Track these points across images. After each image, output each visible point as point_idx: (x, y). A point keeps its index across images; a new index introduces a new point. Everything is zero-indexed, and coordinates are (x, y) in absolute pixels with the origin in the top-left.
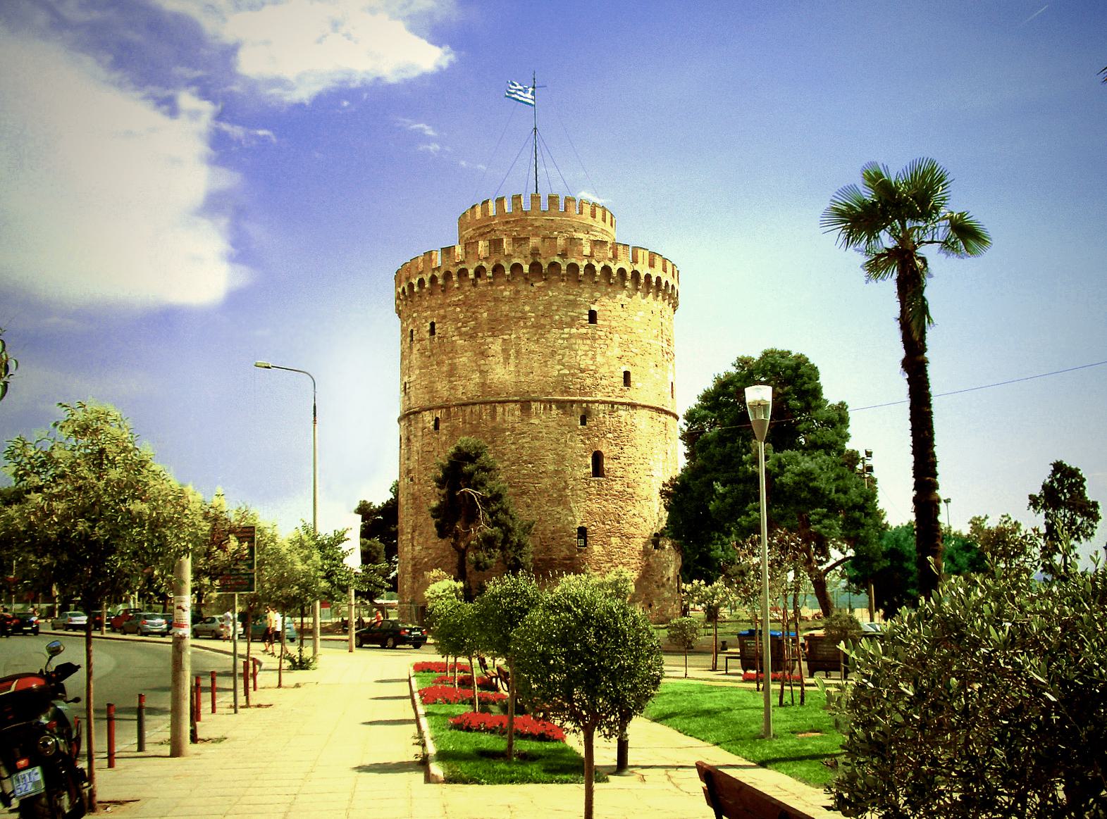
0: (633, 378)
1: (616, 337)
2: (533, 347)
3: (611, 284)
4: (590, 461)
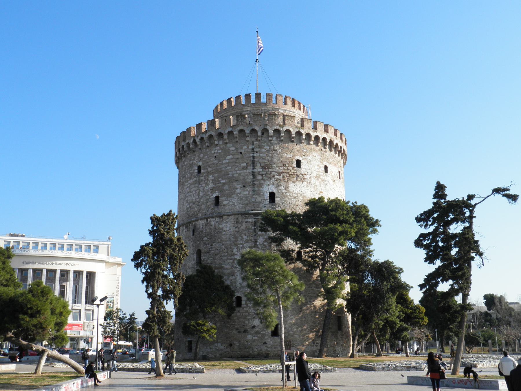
0: (221, 199)
1: (211, 177)
3: (208, 146)
4: (195, 256)
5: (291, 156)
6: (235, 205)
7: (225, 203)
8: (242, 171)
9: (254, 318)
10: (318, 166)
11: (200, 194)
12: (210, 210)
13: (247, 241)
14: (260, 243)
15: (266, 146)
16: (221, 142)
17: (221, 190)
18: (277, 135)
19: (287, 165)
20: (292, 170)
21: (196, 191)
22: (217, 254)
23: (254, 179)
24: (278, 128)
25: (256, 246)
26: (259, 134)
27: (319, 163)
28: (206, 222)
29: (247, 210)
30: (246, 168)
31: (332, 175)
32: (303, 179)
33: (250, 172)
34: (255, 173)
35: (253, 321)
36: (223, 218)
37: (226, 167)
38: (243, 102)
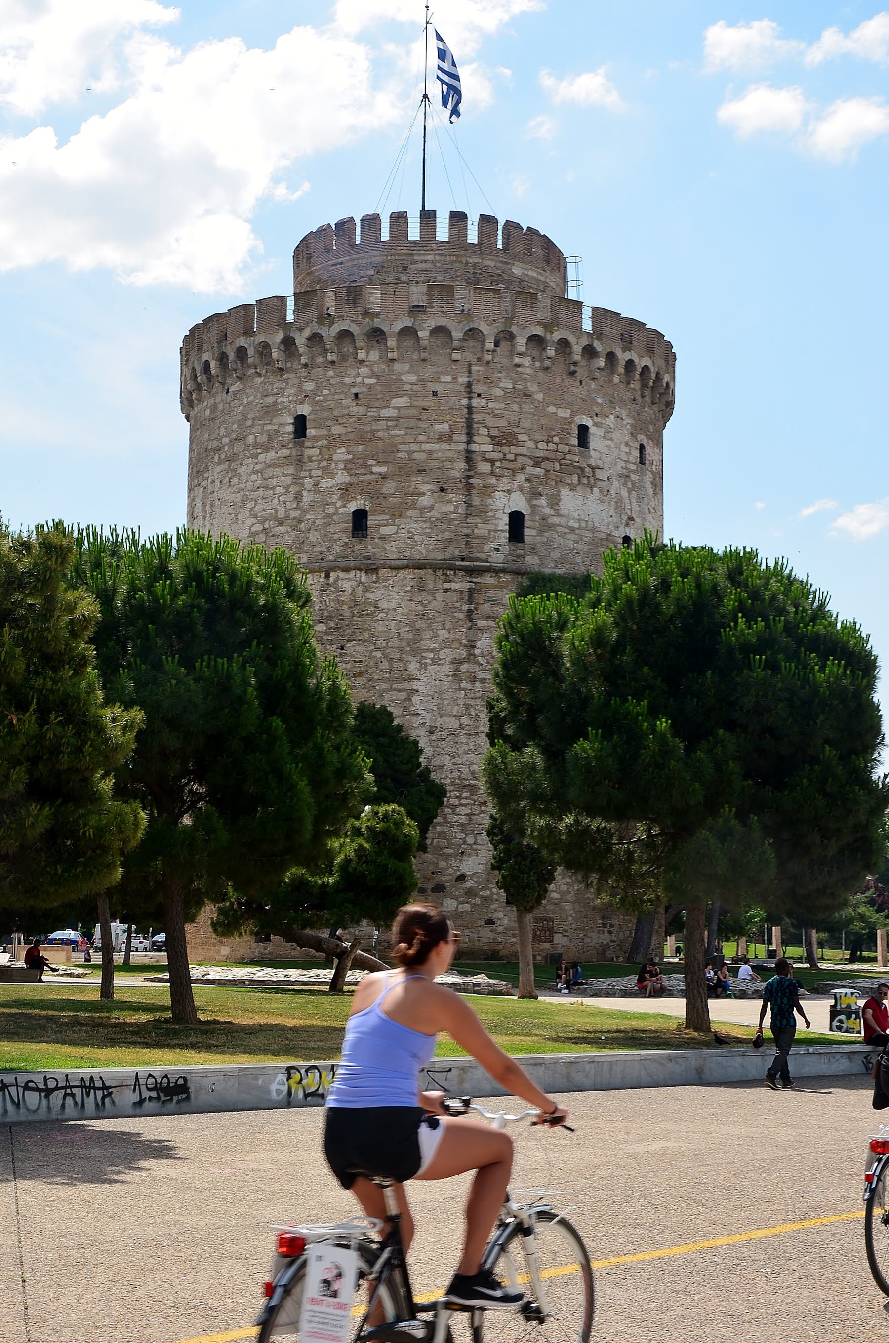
0: (371, 520)
1: (341, 454)
2: (227, 494)
3: (333, 362)
5: (567, 413)
6: (416, 542)
7: (385, 530)
8: (437, 446)
9: (462, 853)
10: (627, 444)
11: (305, 499)
13: (447, 644)
14: (482, 652)
15: (503, 380)
16: (374, 355)
17: (375, 496)
18: (535, 352)
19: (556, 439)
20: (569, 452)
21: (288, 486)
22: (360, 674)
23: (469, 470)
24: (539, 331)
25: (472, 657)
26: (490, 345)
27: (627, 438)
28: (322, 580)
29: (448, 556)
30: (448, 438)
31: (652, 472)
32: (592, 479)
33: (459, 451)
34: (474, 456)
35: (461, 860)
36: (377, 573)
37: (388, 429)
38: (414, 233)
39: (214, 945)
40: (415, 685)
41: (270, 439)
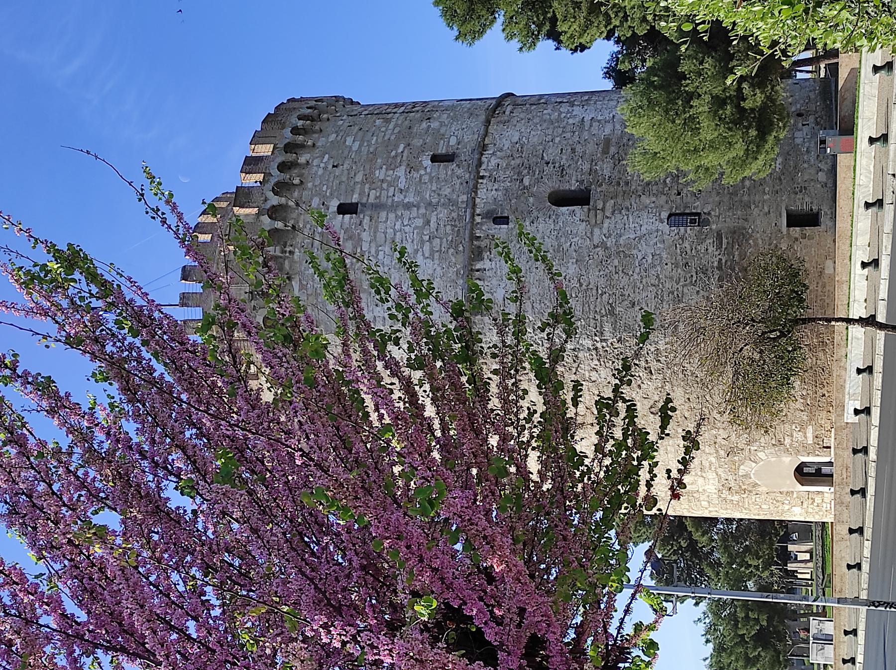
0: (441, 150)
4: (564, 209)
7: (453, 141)
11: (412, 200)
12: (459, 172)
22: (573, 150)
28: (485, 181)
39: (824, 286)
40: (588, 118)
41: (350, 238)
